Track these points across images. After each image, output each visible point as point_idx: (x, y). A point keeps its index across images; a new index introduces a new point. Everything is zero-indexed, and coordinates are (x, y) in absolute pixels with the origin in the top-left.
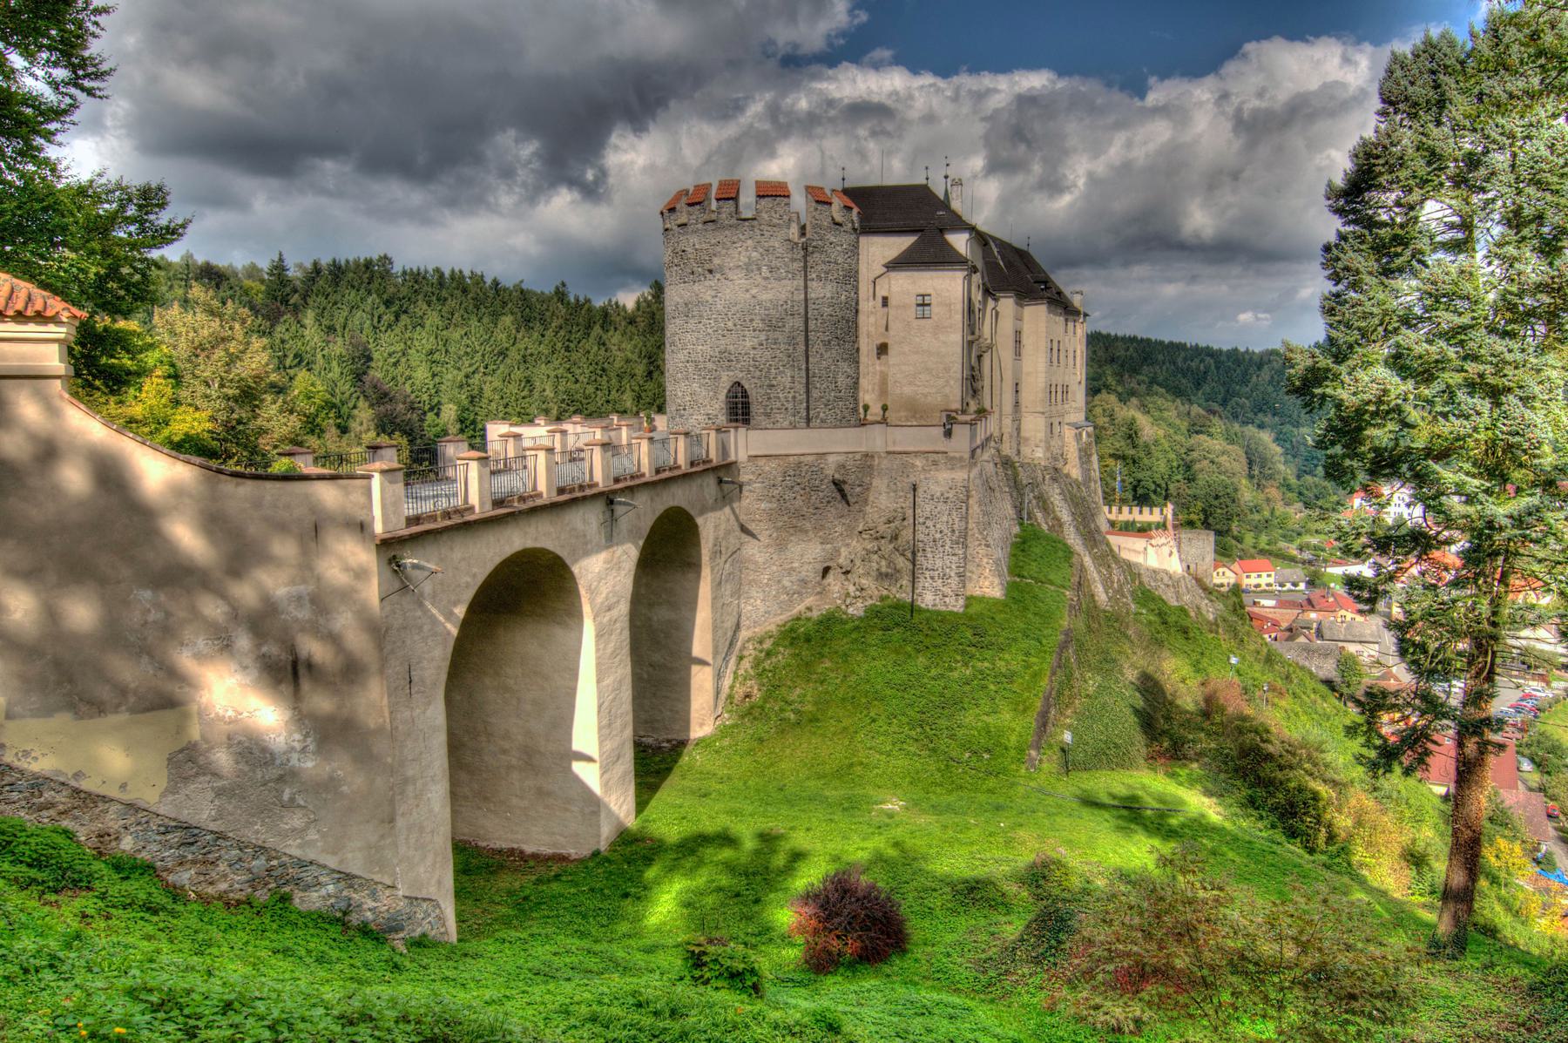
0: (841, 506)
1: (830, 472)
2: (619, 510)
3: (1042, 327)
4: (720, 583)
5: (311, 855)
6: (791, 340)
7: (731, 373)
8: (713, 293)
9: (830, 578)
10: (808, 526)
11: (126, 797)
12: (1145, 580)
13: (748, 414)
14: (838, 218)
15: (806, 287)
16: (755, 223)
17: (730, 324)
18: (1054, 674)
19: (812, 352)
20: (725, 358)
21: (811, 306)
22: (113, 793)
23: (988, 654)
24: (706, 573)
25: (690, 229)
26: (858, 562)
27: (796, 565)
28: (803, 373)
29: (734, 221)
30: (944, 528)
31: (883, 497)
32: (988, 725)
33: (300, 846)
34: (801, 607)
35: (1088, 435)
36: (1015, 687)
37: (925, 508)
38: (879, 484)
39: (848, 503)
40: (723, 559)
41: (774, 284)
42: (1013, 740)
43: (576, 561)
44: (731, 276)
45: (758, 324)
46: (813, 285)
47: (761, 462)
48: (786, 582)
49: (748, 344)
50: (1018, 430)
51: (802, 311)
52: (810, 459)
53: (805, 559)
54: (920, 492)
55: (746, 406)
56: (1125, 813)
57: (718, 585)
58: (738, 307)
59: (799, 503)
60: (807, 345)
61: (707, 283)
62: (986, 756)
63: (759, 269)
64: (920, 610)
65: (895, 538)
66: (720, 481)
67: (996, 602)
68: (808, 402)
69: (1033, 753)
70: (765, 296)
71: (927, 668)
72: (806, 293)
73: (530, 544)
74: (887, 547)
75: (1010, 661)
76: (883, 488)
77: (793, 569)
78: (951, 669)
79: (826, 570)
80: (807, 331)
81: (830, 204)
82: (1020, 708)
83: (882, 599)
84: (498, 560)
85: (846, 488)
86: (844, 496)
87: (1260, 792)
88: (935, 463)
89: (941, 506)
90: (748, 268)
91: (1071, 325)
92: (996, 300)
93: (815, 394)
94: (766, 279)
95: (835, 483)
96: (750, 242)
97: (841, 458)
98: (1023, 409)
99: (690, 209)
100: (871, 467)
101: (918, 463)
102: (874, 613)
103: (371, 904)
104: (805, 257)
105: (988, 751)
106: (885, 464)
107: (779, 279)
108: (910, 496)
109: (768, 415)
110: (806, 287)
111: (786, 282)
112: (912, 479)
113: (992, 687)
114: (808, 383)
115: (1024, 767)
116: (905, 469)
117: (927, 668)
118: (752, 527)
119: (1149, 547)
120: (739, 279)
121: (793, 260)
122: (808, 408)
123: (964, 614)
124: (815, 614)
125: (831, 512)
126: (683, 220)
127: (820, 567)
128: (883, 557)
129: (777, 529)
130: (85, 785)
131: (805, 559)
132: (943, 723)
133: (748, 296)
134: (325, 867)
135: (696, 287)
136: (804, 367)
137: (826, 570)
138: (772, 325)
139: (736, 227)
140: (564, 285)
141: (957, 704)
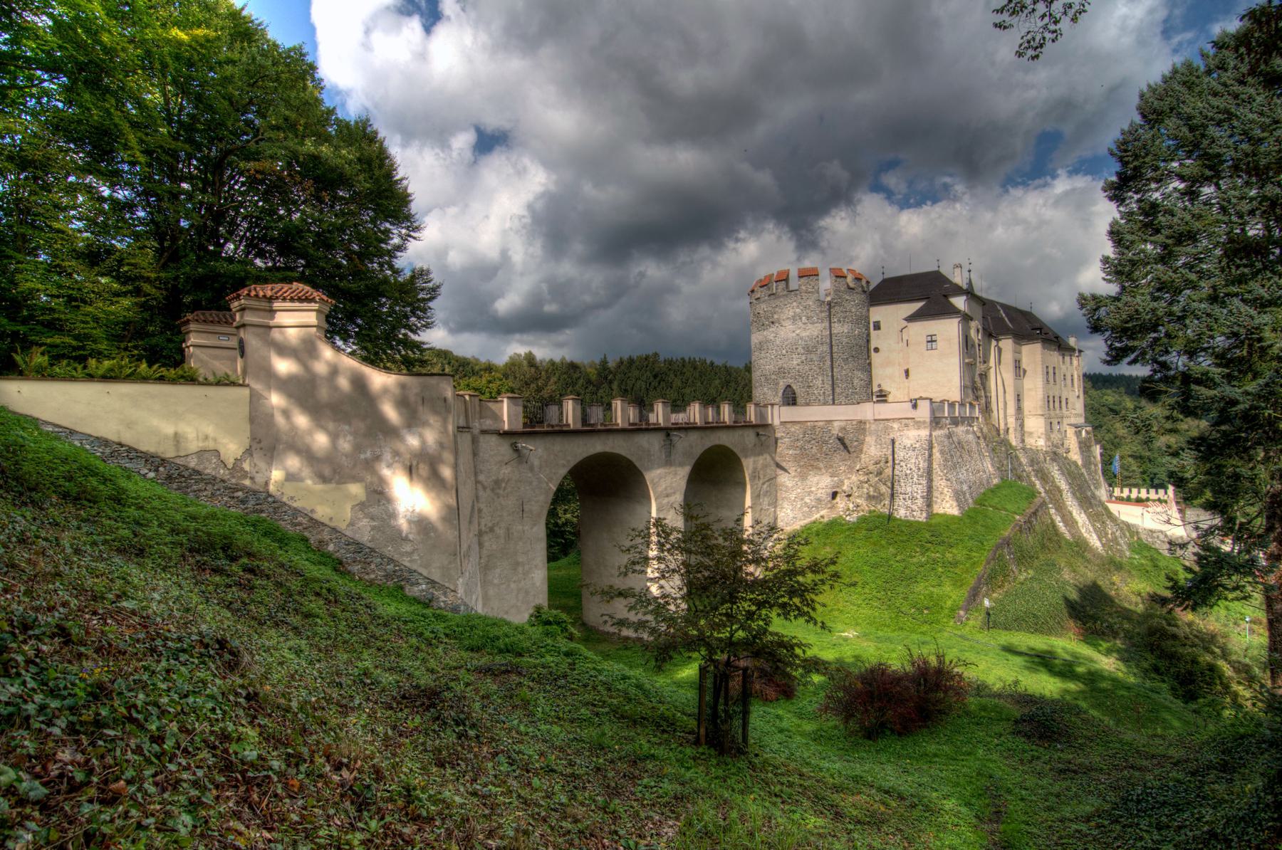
0: (844, 453)
1: (835, 432)
2: (675, 439)
3: (1039, 357)
4: (759, 496)
5: (414, 567)
6: (822, 359)
9: (838, 499)
10: (821, 465)
11: (332, 524)
12: (1143, 537)
14: (852, 285)
15: (830, 327)
18: (988, 563)
19: (836, 365)
21: (834, 338)
22: (327, 522)
23: (941, 548)
24: (748, 487)
26: (855, 489)
27: (813, 489)
29: (785, 293)
30: (913, 467)
31: (873, 448)
32: (932, 593)
33: (410, 561)
34: (818, 516)
35: (1087, 432)
36: (957, 571)
37: (900, 454)
38: (870, 440)
39: (849, 452)
40: (761, 481)
41: (810, 326)
42: (949, 603)
43: (648, 469)
44: (784, 323)
45: (800, 350)
47: (789, 426)
48: (807, 500)
49: (795, 362)
50: (1022, 426)
52: (821, 424)
53: (820, 486)
54: (897, 445)
56: (1037, 660)
57: (756, 497)
59: (814, 450)
60: (832, 361)
62: (925, 612)
64: (896, 519)
65: (879, 473)
66: (758, 434)
67: (953, 517)
69: (962, 613)
70: (804, 334)
71: (895, 556)
73: (608, 449)
74: (874, 479)
75: (958, 553)
76: (873, 443)
77: (812, 492)
78: (912, 557)
79: (834, 495)
80: (832, 353)
81: (845, 277)
82: (958, 583)
83: (870, 512)
84: (585, 455)
85: (847, 442)
86: (845, 447)
87: (1162, 664)
88: (906, 425)
89: (911, 453)
90: (794, 319)
91: (1067, 358)
92: (998, 340)
93: (838, 390)
95: (841, 440)
97: (843, 424)
98: (1026, 412)
100: (864, 429)
101: (896, 425)
102: (863, 520)
103: (443, 598)
104: (830, 309)
105: (927, 608)
106: (873, 427)
108: (890, 447)
110: (830, 327)
112: (892, 436)
113: (940, 569)
115: (952, 621)
116: (887, 430)
117: (895, 556)
118: (784, 464)
119: (1145, 513)
120: (788, 325)
121: (821, 312)
123: (927, 523)
124: (826, 520)
125: (837, 458)
127: (830, 491)
128: (871, 485)
129: (800, 467)
130: (315, 516)
131: (820, 486)
132: (900, 589)
134: (421, 575)
137: (834, 495)
138: (808, 350)
139: (786, 296)
141: (912, 579)
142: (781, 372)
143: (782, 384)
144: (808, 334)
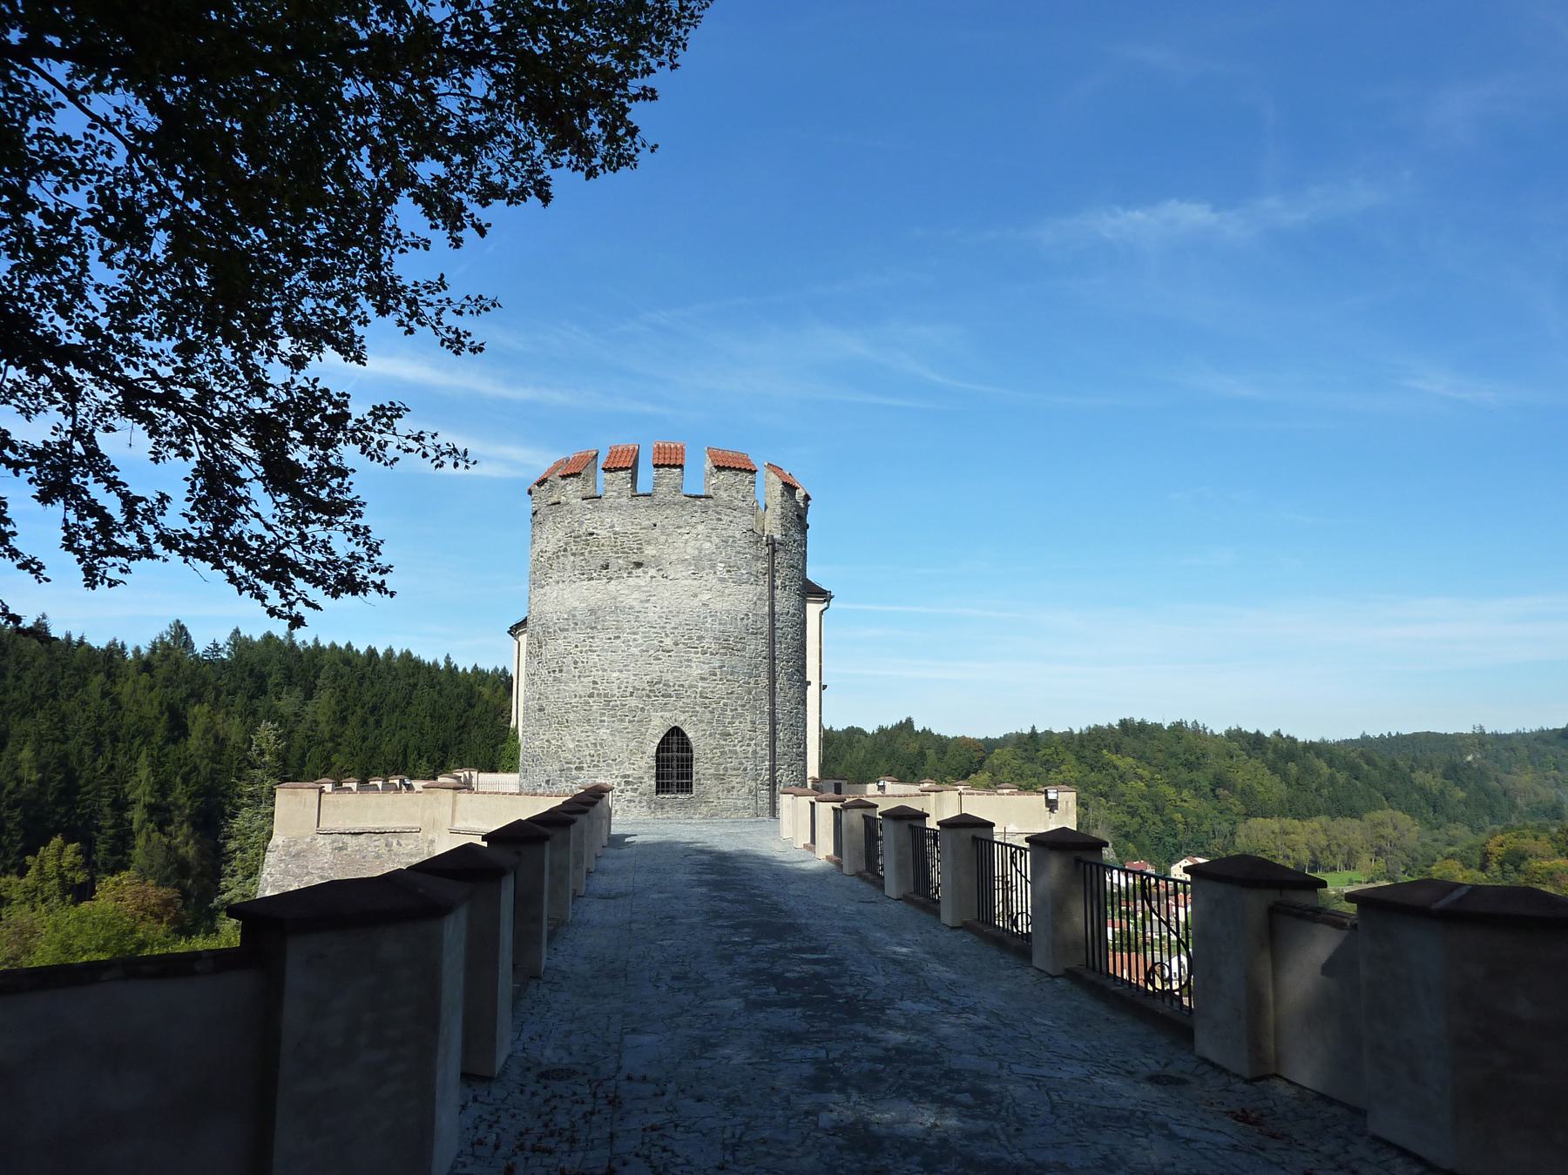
7: (667, 715)
16: (711, 502)
17: (668, 642)
20: (659, 691)
28: (766, 718)
49: (696, 672)
51: (765, 629)
55: (687, 763)
58: (682, 617)
63: (713, 567)
70: (719, 605)
90: (698, 565)
94: (722, 580)
96: (701, 527)
99: (608, 476)
107: (739, 583)
109: (720, 778)
111: (748, 586)
120: (683, 579)
121: (757, 558)
133: (696, 602)
140: (44, 617)
144: (727, 606)
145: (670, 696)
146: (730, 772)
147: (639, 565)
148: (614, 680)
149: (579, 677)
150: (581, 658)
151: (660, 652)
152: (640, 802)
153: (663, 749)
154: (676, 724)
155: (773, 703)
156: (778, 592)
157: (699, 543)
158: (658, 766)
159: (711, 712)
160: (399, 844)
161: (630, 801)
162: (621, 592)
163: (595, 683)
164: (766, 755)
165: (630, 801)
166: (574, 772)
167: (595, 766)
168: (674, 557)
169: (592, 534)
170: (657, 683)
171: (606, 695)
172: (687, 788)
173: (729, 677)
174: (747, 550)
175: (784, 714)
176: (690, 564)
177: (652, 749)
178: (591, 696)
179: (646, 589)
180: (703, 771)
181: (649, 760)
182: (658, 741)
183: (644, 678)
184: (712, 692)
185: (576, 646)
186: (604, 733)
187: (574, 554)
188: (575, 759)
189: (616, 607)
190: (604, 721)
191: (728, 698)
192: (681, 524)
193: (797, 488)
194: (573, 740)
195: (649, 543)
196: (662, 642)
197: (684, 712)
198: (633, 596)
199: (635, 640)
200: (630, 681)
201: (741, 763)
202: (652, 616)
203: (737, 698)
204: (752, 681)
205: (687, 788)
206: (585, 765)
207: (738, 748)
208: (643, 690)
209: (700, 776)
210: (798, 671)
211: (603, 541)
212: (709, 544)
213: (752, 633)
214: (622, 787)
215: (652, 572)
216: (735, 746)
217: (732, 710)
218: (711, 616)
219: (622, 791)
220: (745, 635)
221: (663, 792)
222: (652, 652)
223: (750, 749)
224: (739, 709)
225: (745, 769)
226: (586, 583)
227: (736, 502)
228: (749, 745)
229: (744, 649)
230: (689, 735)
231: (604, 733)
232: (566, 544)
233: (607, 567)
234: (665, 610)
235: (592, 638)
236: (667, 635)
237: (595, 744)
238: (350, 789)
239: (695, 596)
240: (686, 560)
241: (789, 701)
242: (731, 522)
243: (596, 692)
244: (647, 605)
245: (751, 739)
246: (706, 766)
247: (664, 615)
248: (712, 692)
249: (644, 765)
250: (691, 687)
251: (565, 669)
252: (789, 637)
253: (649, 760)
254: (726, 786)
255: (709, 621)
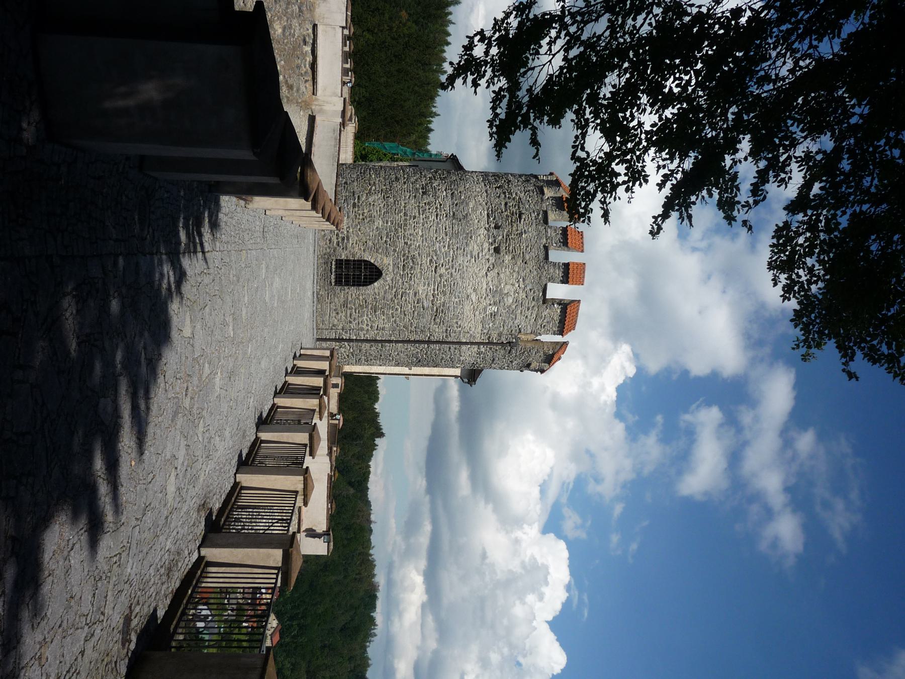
8: (475, 253)
13: (347, 284)
15: (472, 343)
17: (443, 270)
25: (541, 228)
28: (388, 338)
41: (479, 317)
45: (441, 299)
46: (475, 348)
49: (421, 289)
51: (450, 339)
60: (415, 342)
61: (486, 245)
63: (495, 304)
68: (356, 340)
70: (467, 308)
72: (466, 343)
80: (429, 342)
90: (497, 295)
93: (365, 346)
94: (485, 309)
107: (483, 322)
109: (345, 304)
110: (472, 343)
111: (480, 328)
114: (376, 341)
121: (500, 335)
122: (350, 340)
126: (551, 216)
133: (470, 291)
135: (482, 231)
136: (393, 338)
138: (438, 313)
142: (407, 262)
143: (383, 261)
145: (404, 270)
146: (349, 312)
147: (497, 250)
148: (416, 231)
149: (419, 206)
150: (433, 209)
151: (435, 265)
152: (329, 248)
153: (367, 265)
154: (384, 275)
155: (397, 342)
156: (476, 347)
157: (512, 294)
158: (354, 261)
159: (392, 299)
160: (306, 81)
161: (330, 240)
162: (479, 238)
163: (415, 217)
164: (361, 337)
165: (330, 240)
166: (352, 202)
167: (356, 216)
168: (502, 276)
169: (520, 217)
170: (413, 261)
171: (406, 225)
172: (338, 282)
173: (416, 313)
174: (506, 328)
175: (389, 350)
176: (497, 287)
177: (367, 257)
178: (405, 214)
179: (480, 255)
180: (350, 293)
181: (358, 254)
182: (372, 261)
183: (417, 252)
184: (406, 300)
185: (441, 205)
186: (379, 223)
187: (506, 204)
188: (361, 202)
189: (468, 234)
190: (387, 223)
191: (401, 311)
192: (527, 282)
193: (549, 364)
194: (374, 201)
195: (513, 258)
196: (442, 265)
197: (392, 280)
198: (475, 246)
199: (444, 246)
200: (415, 243)
201: (355, 319)
202: (460, 259)
203: (401, 318)
204: (413, 329)
205: (338, 282)
206: (356, 209)
207: (365, 317)
208: (409, 252)
209: (347, 291)
210: (419, 361)
211: (515, 225)
212: (511, 301)
213: (447, 330)
214: (340, 235)
215: (492, 260)
216: (367, 315)
217: (392, 314)
218: (460, 301)
219: (337, 235)
220: (446, 325)
221: (336, 264)
222: (435, 258)
223: (364, 326)
224: (394, 319)
225: (350, 322)
226: (486, 212)
227: (540, 322)
228: (367, 325)
229: (435, 324)
230: (376, 284)
231: (379, 223)
232: (514, 199)
233: (497, 227)
234: (465, 268)
235: (446, 216)
236: (446, 270)
237: (371, 217)
238: (346, 46)
239: (475, 290)
240: (500, 285)
241: (398, 354)
242: (527, 317)
243: (408, 218)
244: (469, 256)
245: (371, 327)
246: (354, 295)
247: (461, 267)
248: (406, 300)
249: (356, 250)
250: (410, 285)
251: (425, 196)
252: (444, 356)
253: (358, 254)
254: (339, 309)
255: (456, 300)
